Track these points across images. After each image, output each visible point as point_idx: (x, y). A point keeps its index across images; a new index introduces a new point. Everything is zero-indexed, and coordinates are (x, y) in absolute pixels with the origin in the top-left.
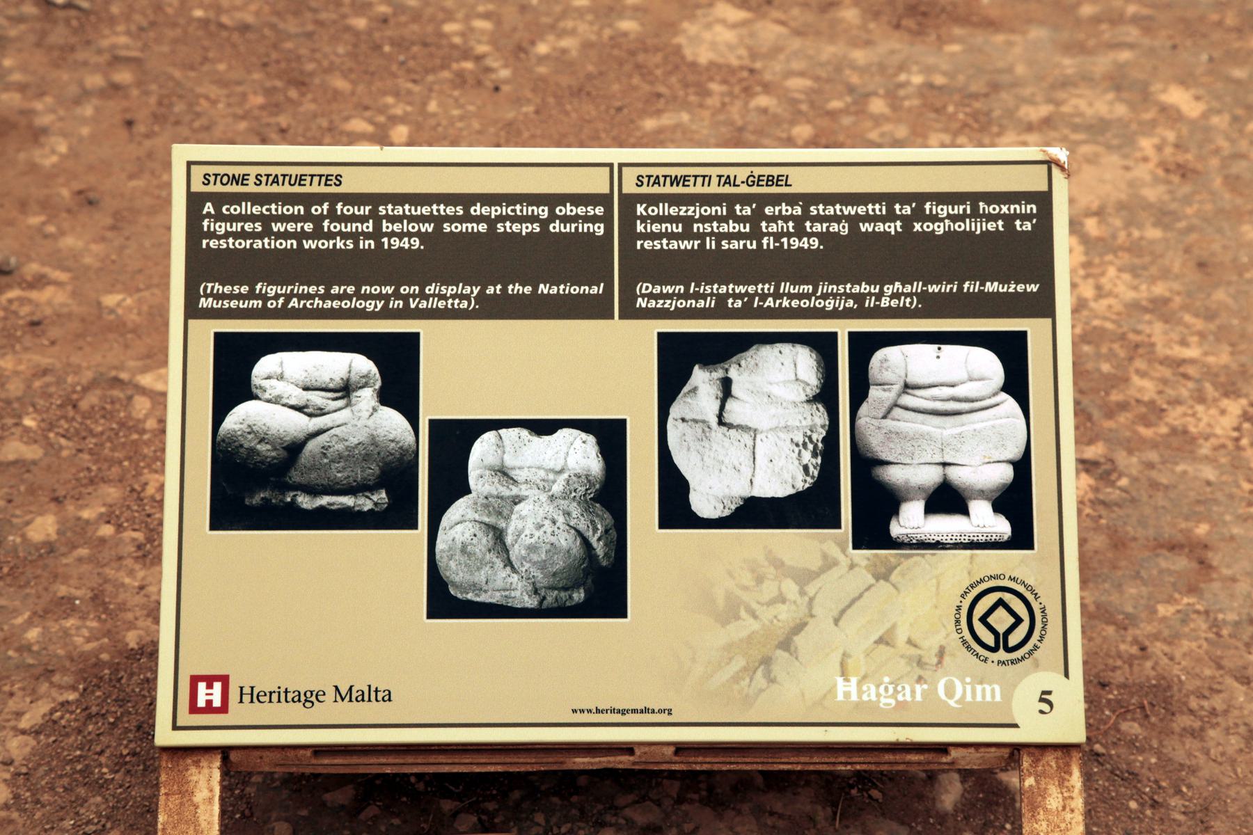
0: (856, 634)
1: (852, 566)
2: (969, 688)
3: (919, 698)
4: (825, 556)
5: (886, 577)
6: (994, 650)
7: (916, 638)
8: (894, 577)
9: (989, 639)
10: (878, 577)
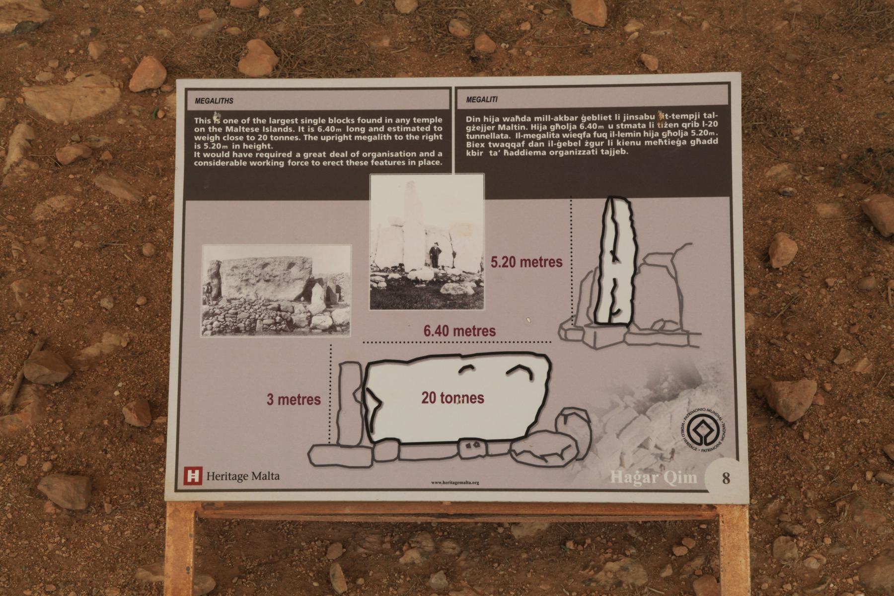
0: (628, 442)
1: (626, 407)
2: (680, 477)
3: (654, 481)
4: (612, 402)
5: (643, 412)
6: (700, 444)
7: (660, 444)
8: (648, 413)
9: (697, 439)
10: (640, 413)
